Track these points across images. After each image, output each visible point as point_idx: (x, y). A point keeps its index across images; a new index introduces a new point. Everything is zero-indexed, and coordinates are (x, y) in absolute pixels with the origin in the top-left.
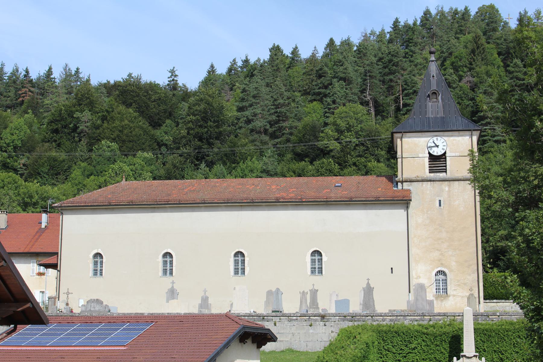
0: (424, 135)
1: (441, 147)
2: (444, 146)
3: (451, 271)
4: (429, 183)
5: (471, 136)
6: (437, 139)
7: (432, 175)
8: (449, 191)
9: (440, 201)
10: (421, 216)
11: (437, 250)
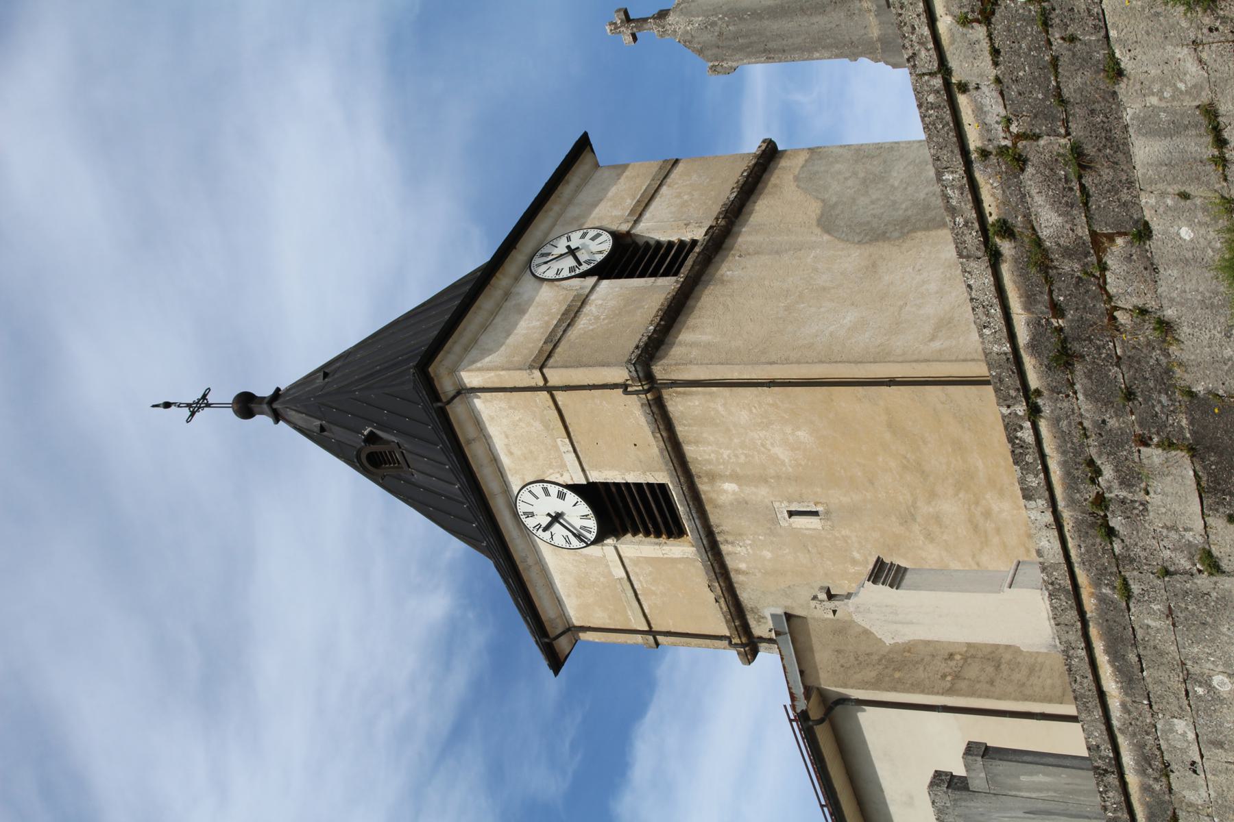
0: (530, 561)
1: (553, 504)
4: (725, 548)
6: (530, 515)
8: (735, 478)
9: (791, 514)
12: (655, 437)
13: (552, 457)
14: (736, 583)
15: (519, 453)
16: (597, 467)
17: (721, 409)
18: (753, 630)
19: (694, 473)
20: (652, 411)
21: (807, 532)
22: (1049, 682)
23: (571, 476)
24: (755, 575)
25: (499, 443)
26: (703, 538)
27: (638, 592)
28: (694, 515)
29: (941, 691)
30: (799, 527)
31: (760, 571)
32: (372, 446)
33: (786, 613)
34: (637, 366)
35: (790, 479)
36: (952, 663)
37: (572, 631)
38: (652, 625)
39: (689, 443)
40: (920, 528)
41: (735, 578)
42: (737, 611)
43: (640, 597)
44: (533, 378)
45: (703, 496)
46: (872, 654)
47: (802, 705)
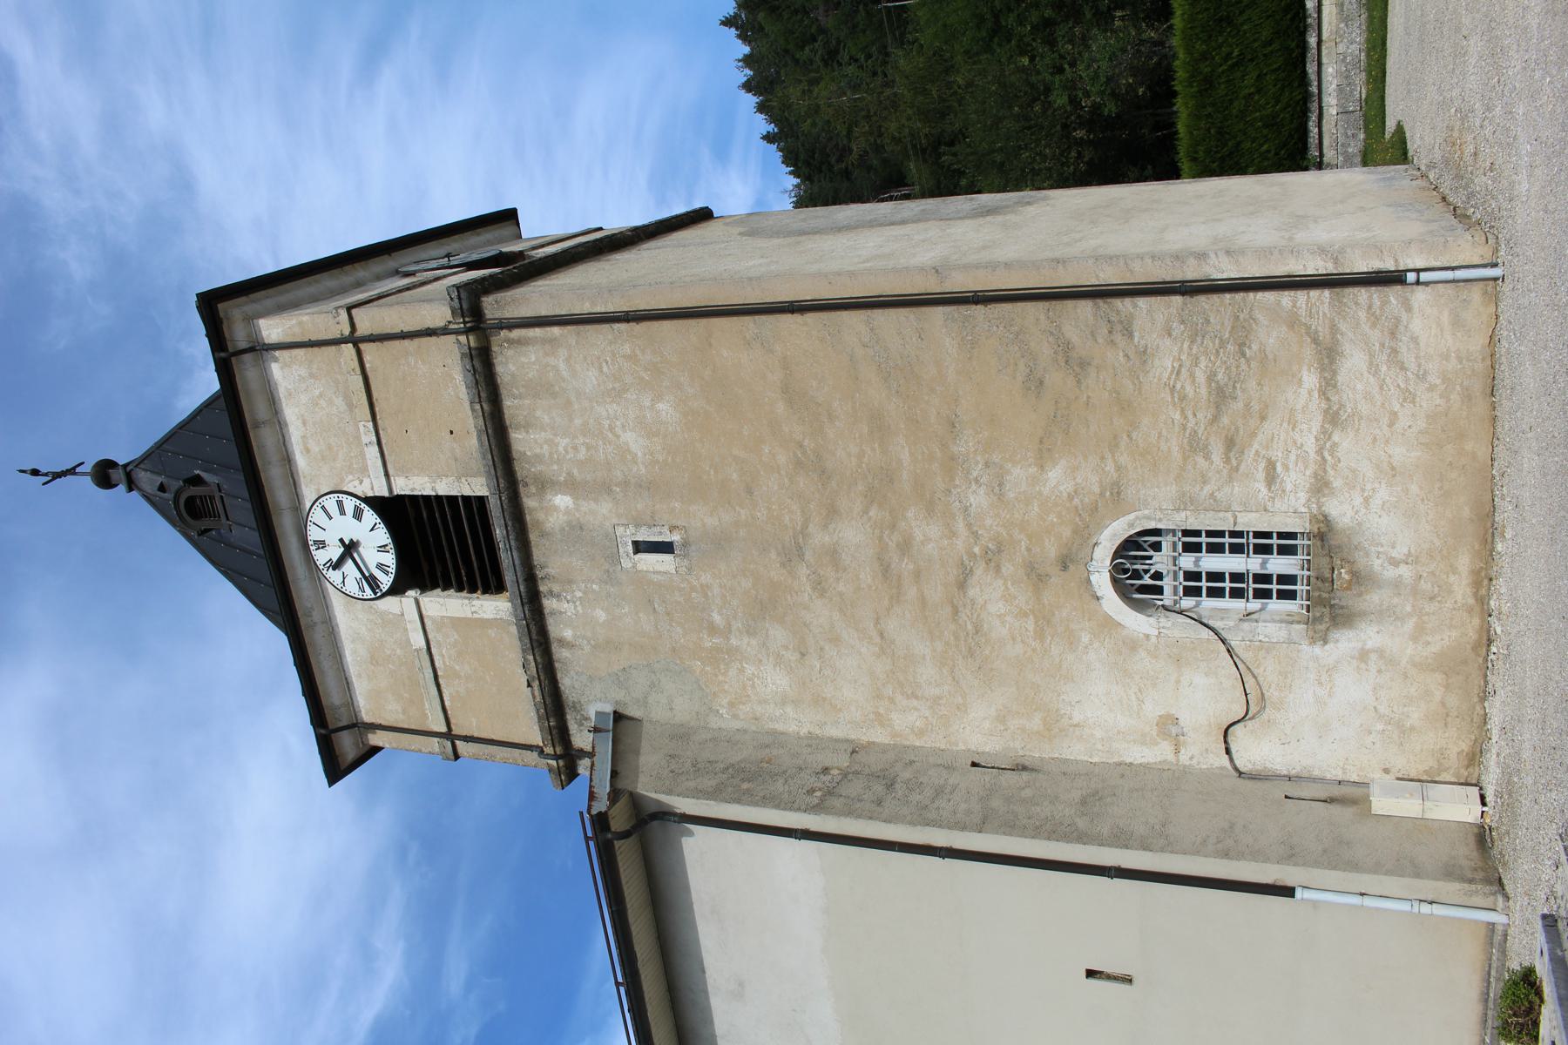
1: (349, 528)
2: (342, 512)
3: (1115, 497)
4: (549, 604)
5: (260, 349)
6: (321, 544)
7: (508, 578)
8: (571, 486)
9: (639, 547)
10: (750, 669)
11: (962, 585)
12: (473, 410)
13: (352, 455)
14: (559, 661)
15: (317, 449)
16: (406, 472)
17: (562, 366)
18: (572, 739)
19: (520, 479)
20: (473, 366)
21: (656, 578)
22: (963, 806)
23: (372, 483)
24: (582, 649)
25: (295, 434)
26: (520, 581)
27: (440, 673)
28: (513, 543)
29: (803, 807)
30: (645, 569)
31: (589, 642)
32: (191, 487)
33: (615, 712)
34: (461, 291)
35: (640, 486)
36: (827, 778)
37: (360, 727)
38: (453, 727)
39: (518, 428)
40: (808, 572)
41: (560, 653)
42: (554, 707)
43: (441, 681)
44: (338, 323)
45: (528, 518)
46: (717, 762)
47: (601, 806)
